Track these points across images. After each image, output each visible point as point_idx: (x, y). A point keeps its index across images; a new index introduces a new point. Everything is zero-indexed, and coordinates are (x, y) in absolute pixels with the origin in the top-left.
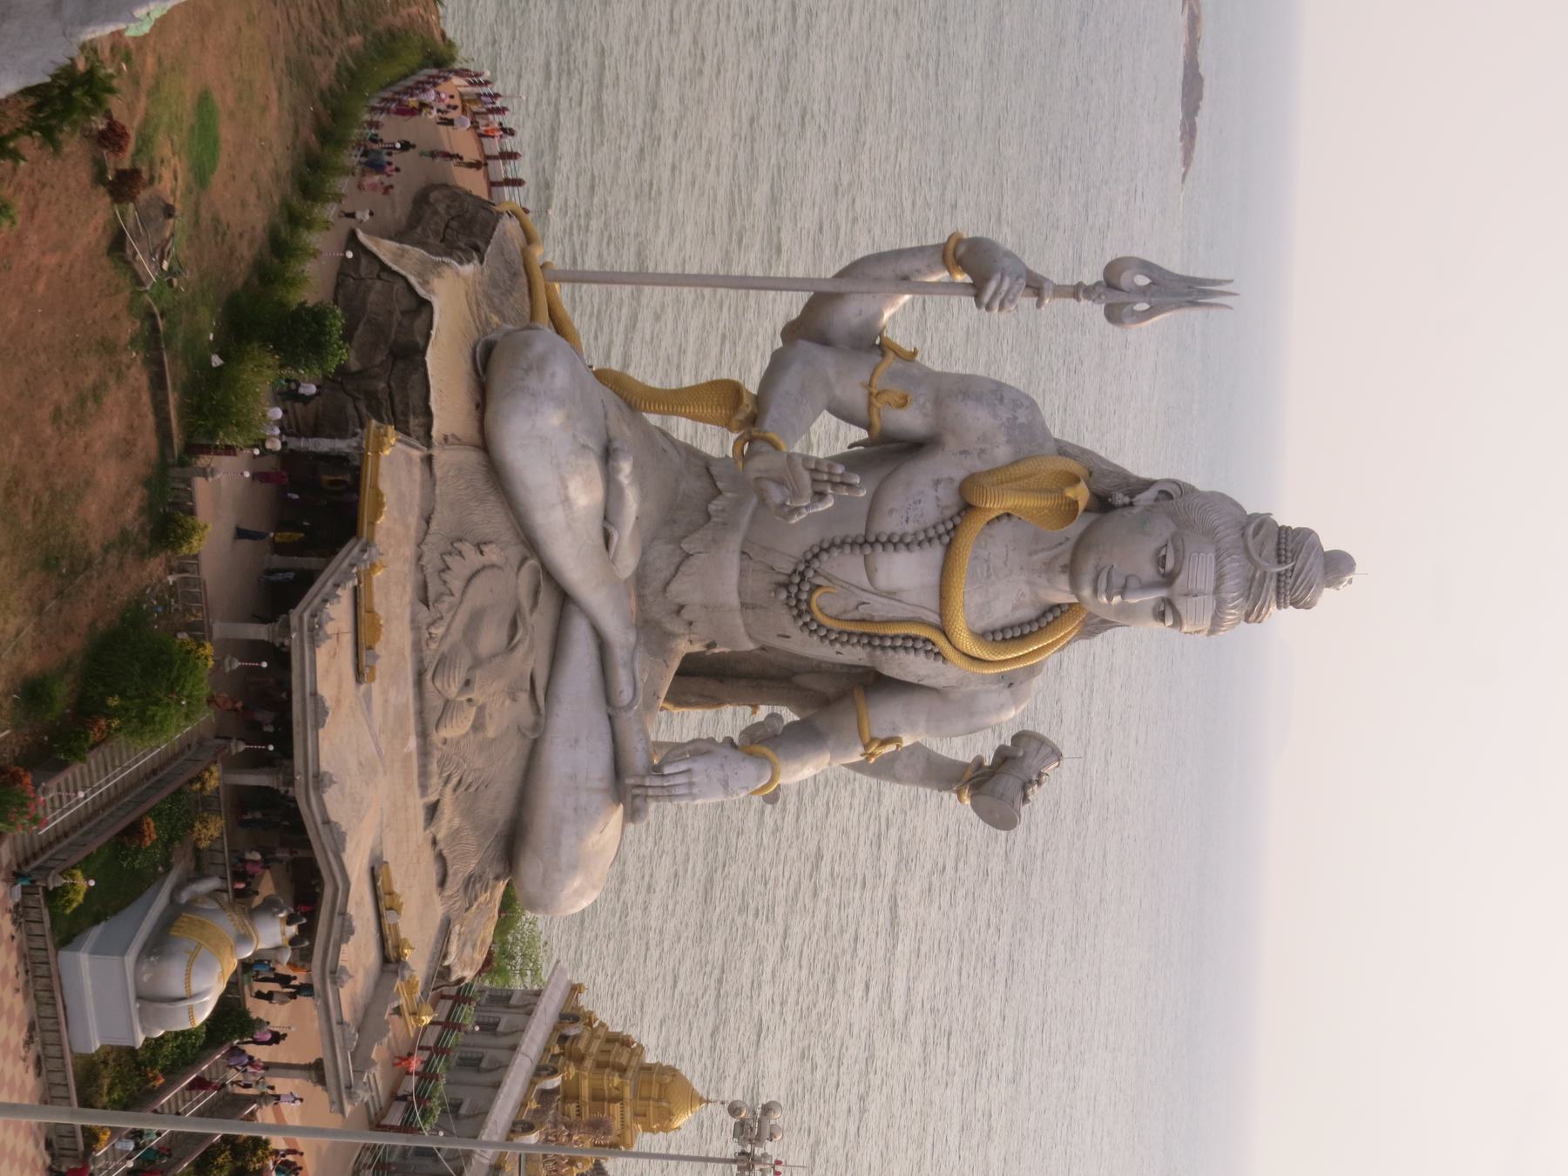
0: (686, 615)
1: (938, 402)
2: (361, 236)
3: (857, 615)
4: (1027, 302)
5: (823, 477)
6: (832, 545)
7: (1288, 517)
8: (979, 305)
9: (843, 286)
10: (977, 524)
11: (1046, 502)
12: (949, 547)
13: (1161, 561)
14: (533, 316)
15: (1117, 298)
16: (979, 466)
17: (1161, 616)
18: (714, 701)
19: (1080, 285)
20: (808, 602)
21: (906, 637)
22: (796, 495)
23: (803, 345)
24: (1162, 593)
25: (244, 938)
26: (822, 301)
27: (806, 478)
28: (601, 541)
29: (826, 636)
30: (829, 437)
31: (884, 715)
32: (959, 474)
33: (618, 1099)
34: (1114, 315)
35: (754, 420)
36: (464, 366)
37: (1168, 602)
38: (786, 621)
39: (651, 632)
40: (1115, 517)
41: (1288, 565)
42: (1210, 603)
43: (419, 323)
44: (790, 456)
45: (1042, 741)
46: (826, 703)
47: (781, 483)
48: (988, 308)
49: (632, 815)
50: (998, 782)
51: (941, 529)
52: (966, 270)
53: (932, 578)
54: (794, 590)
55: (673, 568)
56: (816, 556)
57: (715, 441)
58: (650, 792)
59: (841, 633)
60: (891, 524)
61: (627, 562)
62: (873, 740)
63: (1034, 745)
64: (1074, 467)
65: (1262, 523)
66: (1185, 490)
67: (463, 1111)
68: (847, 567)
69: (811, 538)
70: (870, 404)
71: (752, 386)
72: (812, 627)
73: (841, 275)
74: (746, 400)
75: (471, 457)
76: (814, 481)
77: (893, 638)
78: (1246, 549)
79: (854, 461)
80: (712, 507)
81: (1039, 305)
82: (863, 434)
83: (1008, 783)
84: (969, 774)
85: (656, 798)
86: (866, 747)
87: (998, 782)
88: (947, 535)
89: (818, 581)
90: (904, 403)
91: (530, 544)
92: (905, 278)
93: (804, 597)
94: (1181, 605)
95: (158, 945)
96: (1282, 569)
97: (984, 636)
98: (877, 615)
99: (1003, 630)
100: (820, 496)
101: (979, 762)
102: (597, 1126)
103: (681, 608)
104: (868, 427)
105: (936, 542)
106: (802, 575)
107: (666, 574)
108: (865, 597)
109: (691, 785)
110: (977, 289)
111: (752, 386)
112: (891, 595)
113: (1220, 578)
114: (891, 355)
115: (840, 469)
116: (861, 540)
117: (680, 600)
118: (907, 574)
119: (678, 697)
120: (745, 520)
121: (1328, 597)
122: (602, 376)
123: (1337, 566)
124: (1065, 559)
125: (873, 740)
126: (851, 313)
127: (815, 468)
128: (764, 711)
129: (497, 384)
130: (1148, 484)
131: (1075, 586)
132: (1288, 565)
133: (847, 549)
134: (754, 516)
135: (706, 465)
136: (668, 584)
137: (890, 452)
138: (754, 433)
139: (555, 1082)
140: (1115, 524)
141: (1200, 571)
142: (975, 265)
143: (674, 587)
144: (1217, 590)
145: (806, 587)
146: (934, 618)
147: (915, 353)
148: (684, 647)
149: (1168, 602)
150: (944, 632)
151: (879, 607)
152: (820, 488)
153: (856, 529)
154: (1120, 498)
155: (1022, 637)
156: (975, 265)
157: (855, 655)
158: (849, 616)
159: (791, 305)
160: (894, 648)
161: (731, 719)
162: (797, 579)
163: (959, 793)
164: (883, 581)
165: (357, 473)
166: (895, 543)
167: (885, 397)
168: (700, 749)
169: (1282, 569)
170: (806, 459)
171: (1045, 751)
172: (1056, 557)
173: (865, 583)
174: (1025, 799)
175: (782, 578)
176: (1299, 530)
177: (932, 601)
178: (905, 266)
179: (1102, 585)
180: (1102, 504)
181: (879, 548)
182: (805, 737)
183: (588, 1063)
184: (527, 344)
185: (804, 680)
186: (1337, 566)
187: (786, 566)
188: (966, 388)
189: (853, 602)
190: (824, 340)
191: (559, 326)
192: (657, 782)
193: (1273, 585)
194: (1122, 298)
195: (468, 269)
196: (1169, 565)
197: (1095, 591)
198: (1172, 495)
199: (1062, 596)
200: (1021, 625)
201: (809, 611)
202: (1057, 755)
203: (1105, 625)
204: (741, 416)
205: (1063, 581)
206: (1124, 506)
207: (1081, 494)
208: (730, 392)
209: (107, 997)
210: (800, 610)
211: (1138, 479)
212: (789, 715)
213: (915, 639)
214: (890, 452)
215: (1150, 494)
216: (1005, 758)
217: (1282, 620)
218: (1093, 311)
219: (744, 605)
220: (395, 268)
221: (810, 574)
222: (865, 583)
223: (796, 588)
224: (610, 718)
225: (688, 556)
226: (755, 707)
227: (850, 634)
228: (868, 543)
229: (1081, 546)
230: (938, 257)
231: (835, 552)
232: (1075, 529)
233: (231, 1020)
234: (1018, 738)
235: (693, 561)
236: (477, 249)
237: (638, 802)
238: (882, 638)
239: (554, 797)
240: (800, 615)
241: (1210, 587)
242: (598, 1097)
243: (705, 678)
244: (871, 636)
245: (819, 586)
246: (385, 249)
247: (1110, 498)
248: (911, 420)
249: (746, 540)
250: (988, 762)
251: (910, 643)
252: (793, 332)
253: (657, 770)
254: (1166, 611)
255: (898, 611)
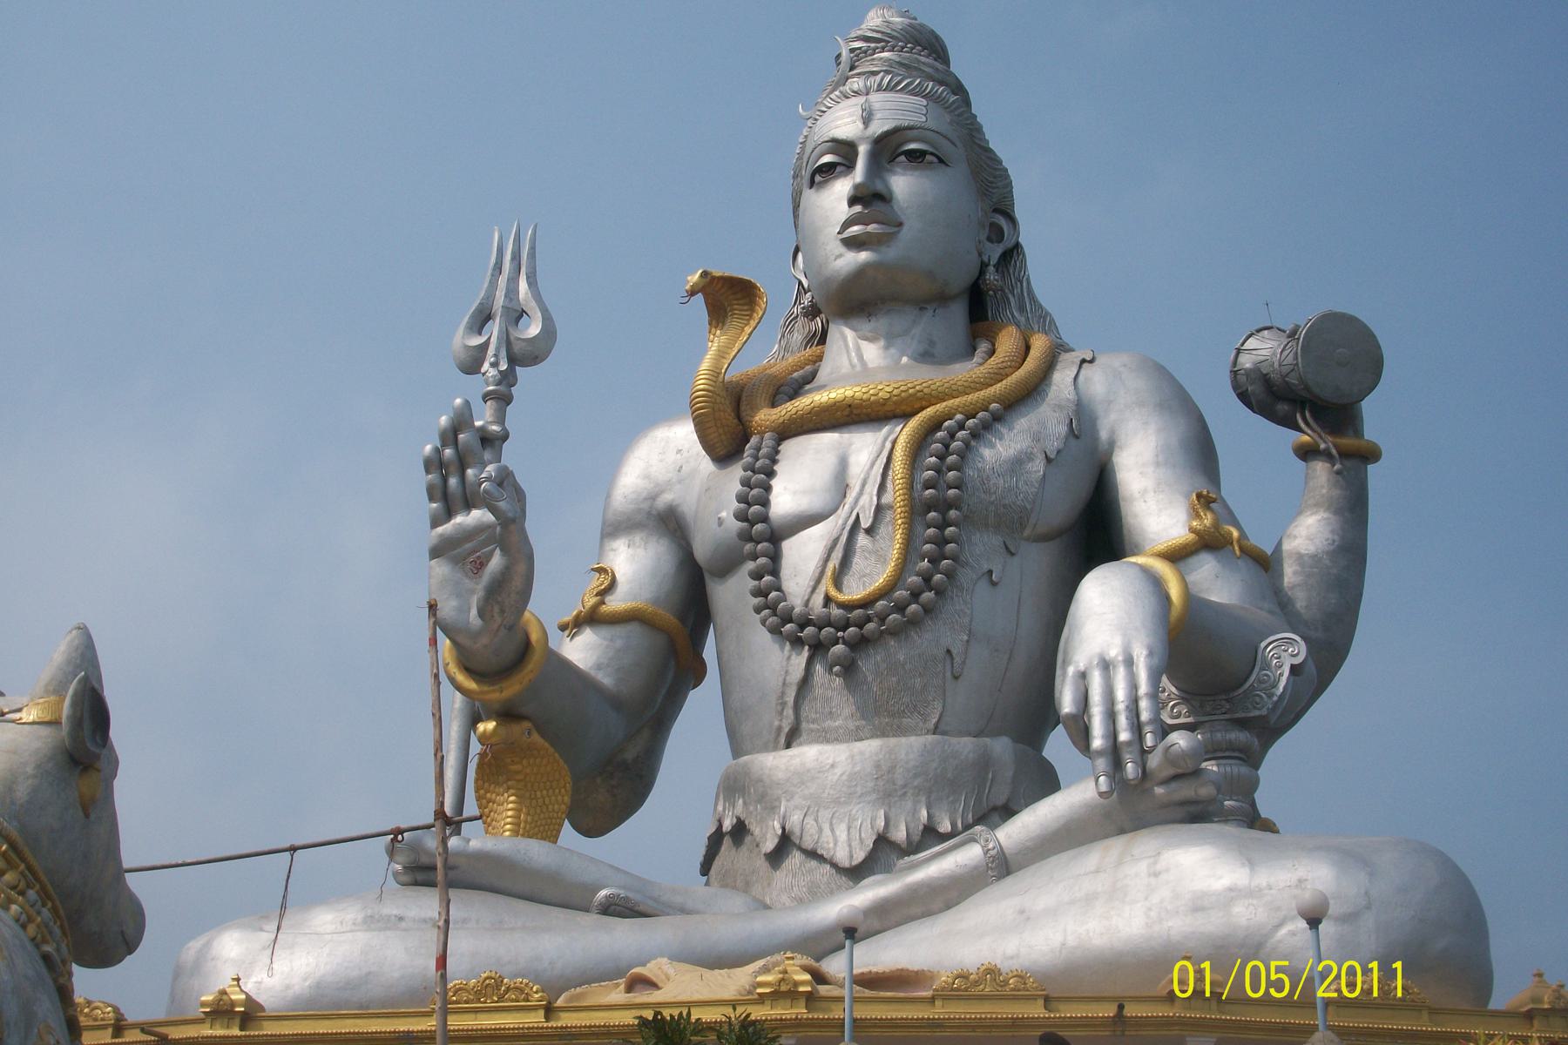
0: (900, 834)
6: (757, 593)
13: (827, 172)
24: (863, 149)
47: (480, 565)
55: (814, 863)
56: (773, 607)
58: (1124, 736)
76: (468, 506)
89: (818, 599)
94: (879, 127)
106: (804, 622)
116: (749, 547)
125: (1192, 530)
136: (834, 865)
143: (842, 856)
144: (857, 93)
150: (923, 409)
162: (809, 630)
187: (800, 660)
196: (827, 159)
221: (797, 610)
228: (763, 537)
235: (795, 819)
241: (861, 99)
245: (828, 600)
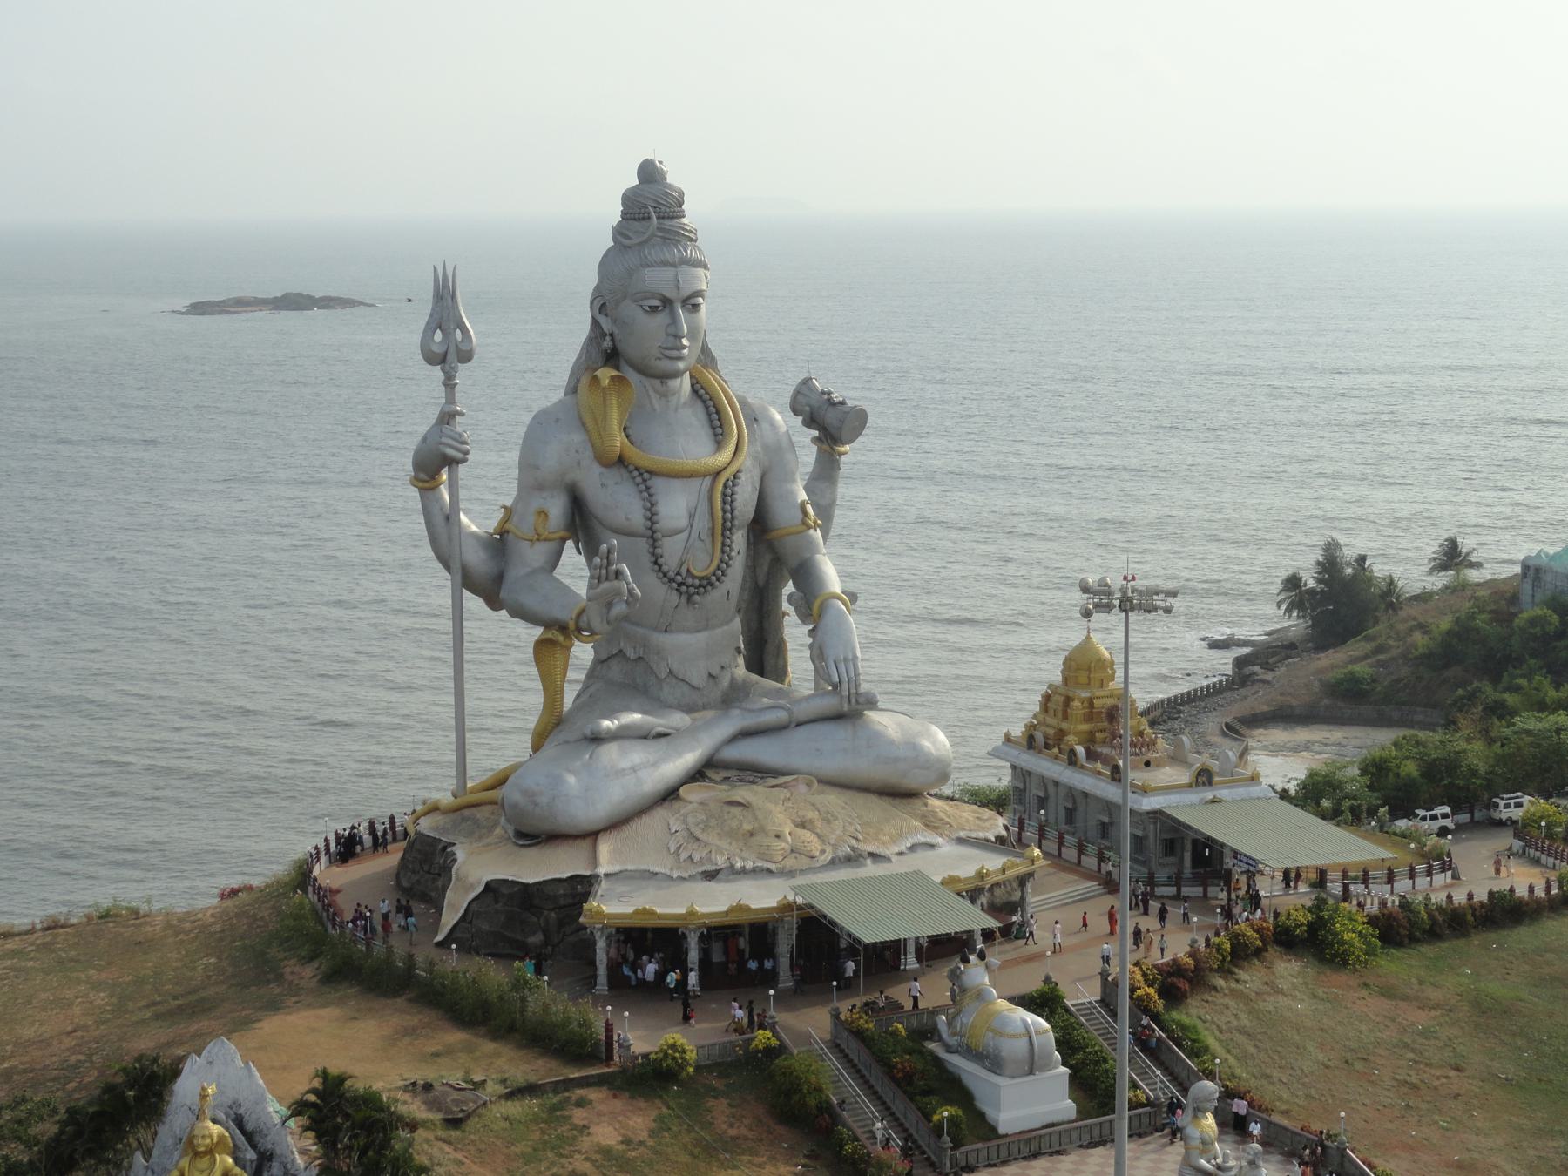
0: (716, 671)
1: (540, 487)
2: (439, 938)
3: (708, 541)
4: (460, 424)
5: (604, 574)
6: (656, 563)
7: (615, 213)
8: (465, 460)
9: (456, 567)
10: (634, 454)
11: (614, 400)
12: (651, 473)
13: (654, 309)
14: (494, 803)
15: (452, 356)
16: (589, 453)
17: (696, 307)
18: (781, 648)
19: (445, 384)
20: (701, 578)
21: (724, 502)
22: (618, 593)
23: (503, 595)
25: (980, 995)
26: (468, 581)
27: (605, 585)
28: (663, 740)
29: (724, 564)
30: (574, 569)
31: (783, 517)
32: (597, 469)
33: (1091, 701)
34: (466, 356)
35: (563, 628)
36: (533, 852)
37: (685, 302)
38: (716, 595)
39: (733, 697)
40: (621, 347)
41: (651, 210)
42: (685, 269)
43: (504, 890)
44: (589, 599)
45: (797, 393)
46: (778, 560)
47: (609, 605)
48: (467, 453)
49: (872, 703)
50: (830, 423)
51: (639, 480)
52: (438, 472)
53: (676, 483)
54: (692, 590)
57: (583, 653)
59: (723, 552)
60: (638, 519)
61: (678, 719)
62: (804, 523)
63: (800, 398)
64: (585, 380)
65: (619, 232)
66: (598, 293)
67: (1106, 820)
68: (672, 550)
69: (652, 579)
70: (546, 540)
71: (538, 631)
72: (720, 573)
73: (448, 568)
74: (549, 635)
75: (605, 848)
77: (724, 512)
78: (640, 244)
79: (591, 550)
80: (632, 656)
81: (461, 414)
82: (570, 543)
83: (831, 417)
84: (825, 447)
85: (857, 686)
86: (809, 527)
87: (830, 423)
88: (644, 477)
89: (684, 572)
90: (543, 514)
91: (670, 795)
92: (448, 518)
93: (697, 582)
94: (686, 292)
95: (993, 1062)
96: (654, 216)
97: (719, 444)
98: (707, 525)
99: (714, 428)
100: (618, 574)
101: (816, 440)
102: (1112, 715)
103: (710, 675)
104: (563, 540)
105: (649, 483)
106: (680, 584)
107: (686, 688)
108: (694, 535)
109: (846, 660)
110: (452, 462)
111: (538, 631)
112: (691, 517)
113: (664, 264)
114: (507, 526)
115: (597, 560)
117: (705, 676)
118: (676, 505)
119: (780, 674)
120: (641, 630)
121: (673, 178)
122: (537, 747)
123: (649, 172)
124: (657, 382)
126: (476, 558)
127: (596, 580)
128: (786, 606)
129: (546, 826)
130: (595, 322)
131: (676, 374)
132: (651, 210)
133: (659, 551)
134: (638, 624)
135: (599, 662)
137: (581, 522)
138: (572, 625)
139: (1080, 750)
140: (629, 348)
141: (658, 280)
142: (434, 463)
143: (695, 682)
144: (674, 265)
145: (690, 581)
146: (708, 481)
147: (505, 507)
148: (741, 671)
149: (685, 302)
150: (718, 473)
151: (702, 524)
152: (612, 575)
153: (643, 544)
154: (607, 344)
155: (718, 412)
156: (434, 463)
157: (739, 539)
158: (709, 547)
159: (474, 603)
160: (732, 511)
161: (795, 633)
162: (684, 588)
163: (841, 454)
164: (684, 522)
165: (618, 930)
166: (651, 515)
167: (541, 530)
168: (818, 654)
169: (654, 216)
170: (590, 587)
171: (805, 391)
172: (656, 392)
173: (684, 535)
174: (842, 403)
175: (684, 599)
176: (623, 204)
177: (696, 483)
178: (439, 520)
179: (674, 353)
180: (613, 357)
181: (657, 526)
182: (806, 576)
183: (1064, 726)
184: (515, 806)
185: (761, 579)
186: (649, 172)
187: (675, 596)
188: (527, 464)
189: (699, 544)
190: (499, 578)
191: (500, 781)
192: (845, 686)
193: (667, 222)
194: (452, 350)
195: (460, 853)
196: (656, 303)
197: (680, 358)
198: (602, 304)
199: (685, 383)
200: (709, 414)
201: (707, 578)
202: (807, 382)
203: (705, 350)
204: (561, 638)
205: (674, 383)
206: (613, 340)
207: (606, 374)
208: (542, 646)
209: (1032, 1099)
210: (706, 584)
211: (592, 330)
212: (789, 588)
213: (724, 495)
214: (581, 522)
215: (602, 320)
216: (812, 421)
217: (694, 213)
218: (463, 374)
219: (706, 628)
220: (462, 911)
221: (679, 578)
222: (684, 535)
223: (690, 587)
224: (799, 724)
225: (671, 672)
226: (784, 614)
227: (723, 545)
228: (652, 535)
229: (644, 371)
230: (429, 494)
231: (661, 561)
232: (633, 377)
233: (1044, 1002)
234: (796, 412)
235: (675, 668)
236: (445, 848)
237: (861, 700)
238: (724, 520)
239: (863, 767)
240: (711, 584)
241: (671, 270)
242: (1090, 716)
243: (763, 653)
244: (724, 528)
246: (449, 919)
247: (608, 352)
248: (557, 508)
249: (656, 629)
250: (816, 433)
251: (728, 498)
252: (494, 603)
253: (836, 687)
254: (691, 303)
255: (703, 508)
